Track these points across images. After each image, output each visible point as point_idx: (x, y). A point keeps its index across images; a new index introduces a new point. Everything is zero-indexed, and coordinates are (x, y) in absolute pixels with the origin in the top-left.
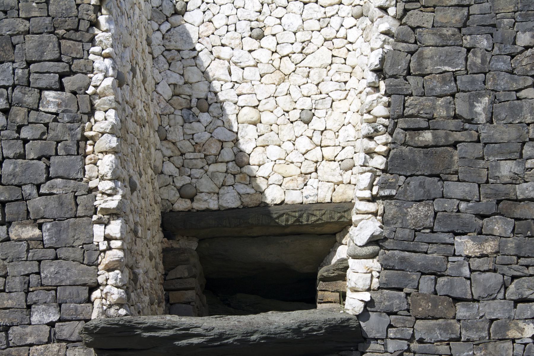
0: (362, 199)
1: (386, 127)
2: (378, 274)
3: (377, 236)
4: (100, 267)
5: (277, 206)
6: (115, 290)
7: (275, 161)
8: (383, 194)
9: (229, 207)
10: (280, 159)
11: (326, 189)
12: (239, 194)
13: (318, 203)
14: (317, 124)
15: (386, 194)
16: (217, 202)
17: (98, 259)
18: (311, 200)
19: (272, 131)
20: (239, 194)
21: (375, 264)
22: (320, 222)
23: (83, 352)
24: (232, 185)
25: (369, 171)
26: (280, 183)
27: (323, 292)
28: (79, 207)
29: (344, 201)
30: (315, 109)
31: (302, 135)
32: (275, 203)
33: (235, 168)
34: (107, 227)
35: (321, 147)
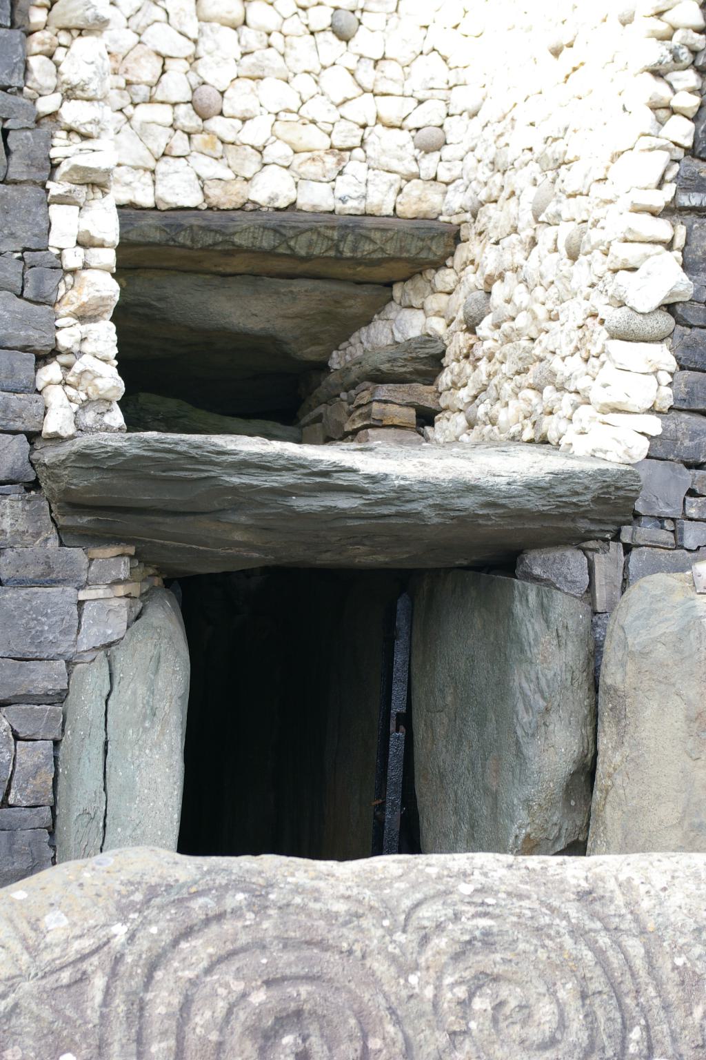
0: (638, 210)
1: (695, 53)
2: (671, 380)
3: (678, 294)
4: (63, 310)
5: (279, 213)
6: (99, 367)
7: (277, 114)
8: (687, 204)
9: (180, 204)
10: (288, 111)
11: (385, 188)
12: (199, 177)
13: (365, 215)
14: (364, 42)
15: (693, 204)
16: (151, 190)
17: (58, 289)
18: (353, 206)
19: (269, 46)
20: (199, 177)
21: (663, 356)
22: (379, 255)
23: (23, 510)
24: (184, 157)
25: (662, 148)
26: (287, 164)
27: (384, 405)
28: (14, 158)
29: (421, 215)
30: (362, 10)
31: (334, 64)
32: (277, 204)
33: (191, 118)
34: (87, 215)
35: (375, 95)
